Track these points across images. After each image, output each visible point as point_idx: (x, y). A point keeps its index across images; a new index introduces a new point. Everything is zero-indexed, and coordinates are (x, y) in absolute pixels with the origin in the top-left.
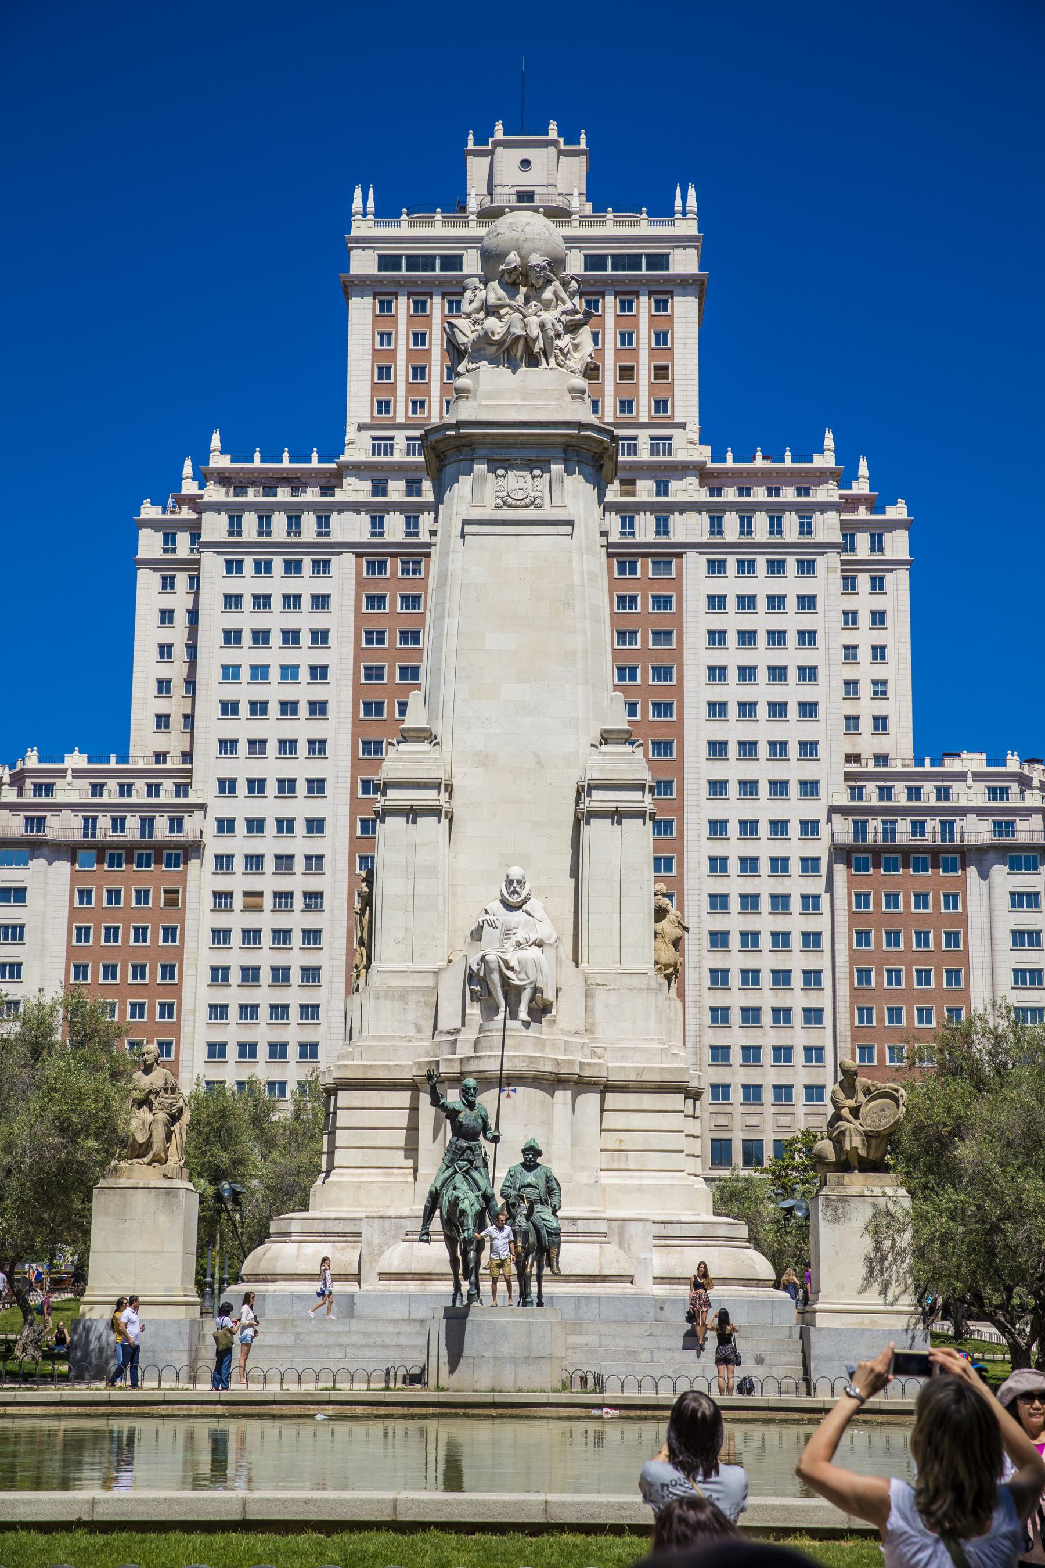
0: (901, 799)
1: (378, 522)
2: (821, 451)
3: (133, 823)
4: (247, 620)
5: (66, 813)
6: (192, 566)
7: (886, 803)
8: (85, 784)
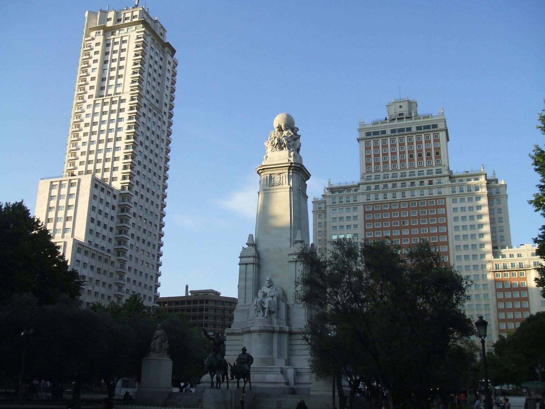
4: (338, 224)
6: (325, 212)
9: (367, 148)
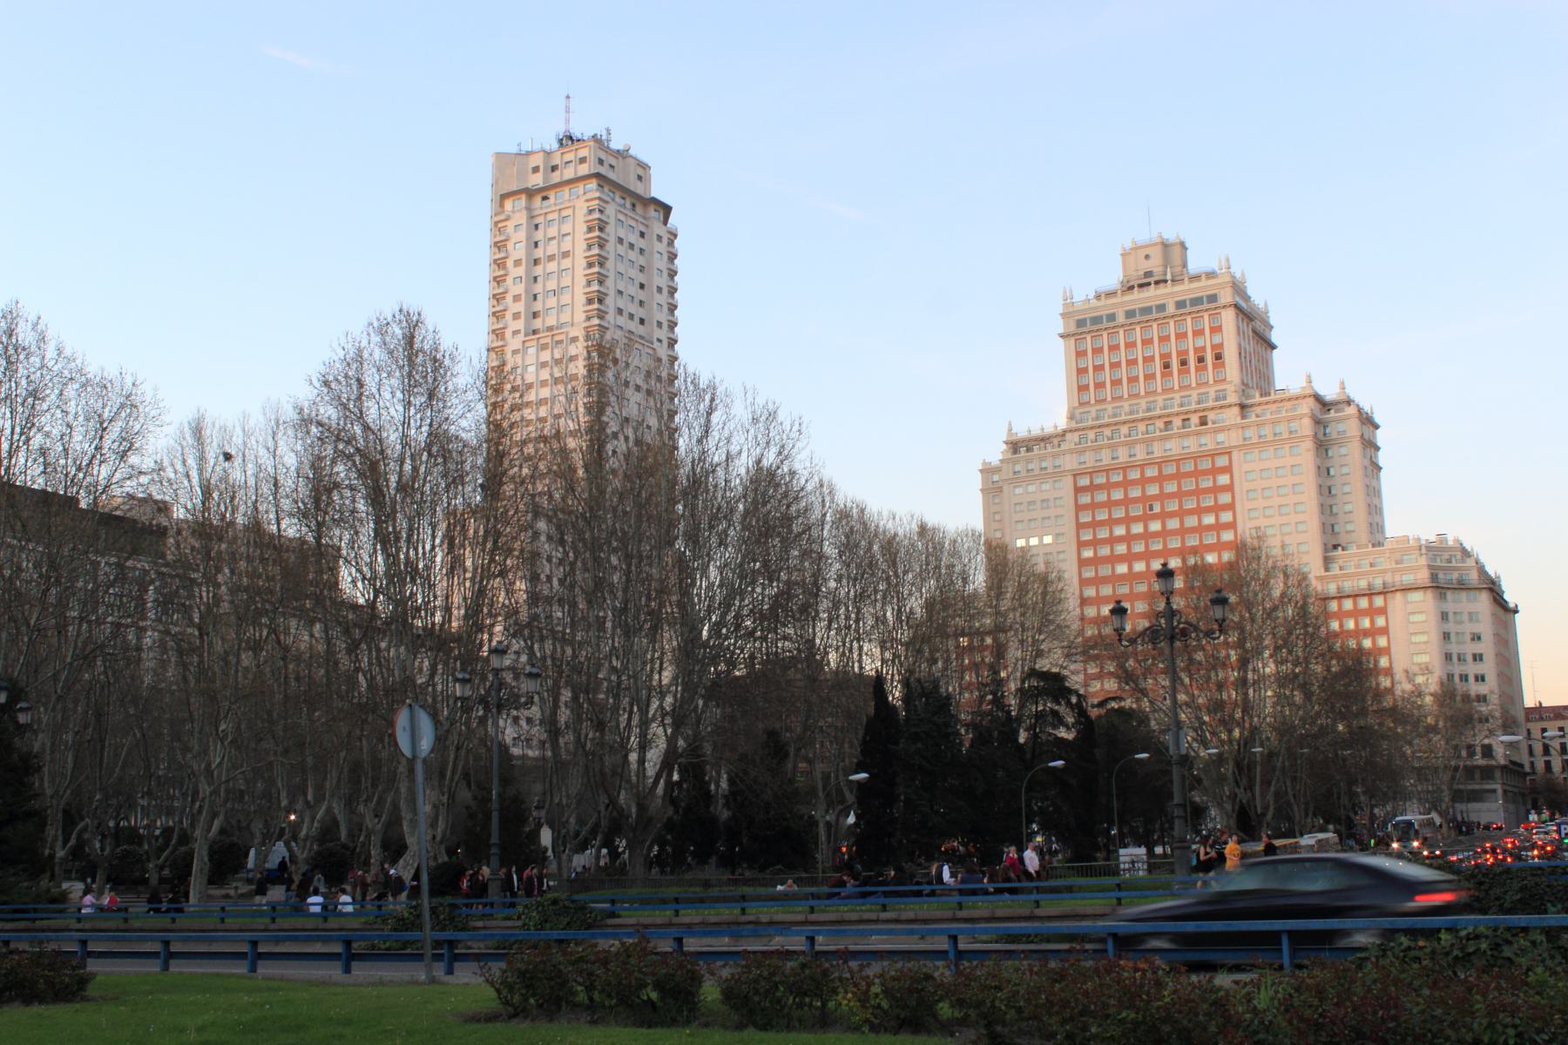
9: (1080, 354)
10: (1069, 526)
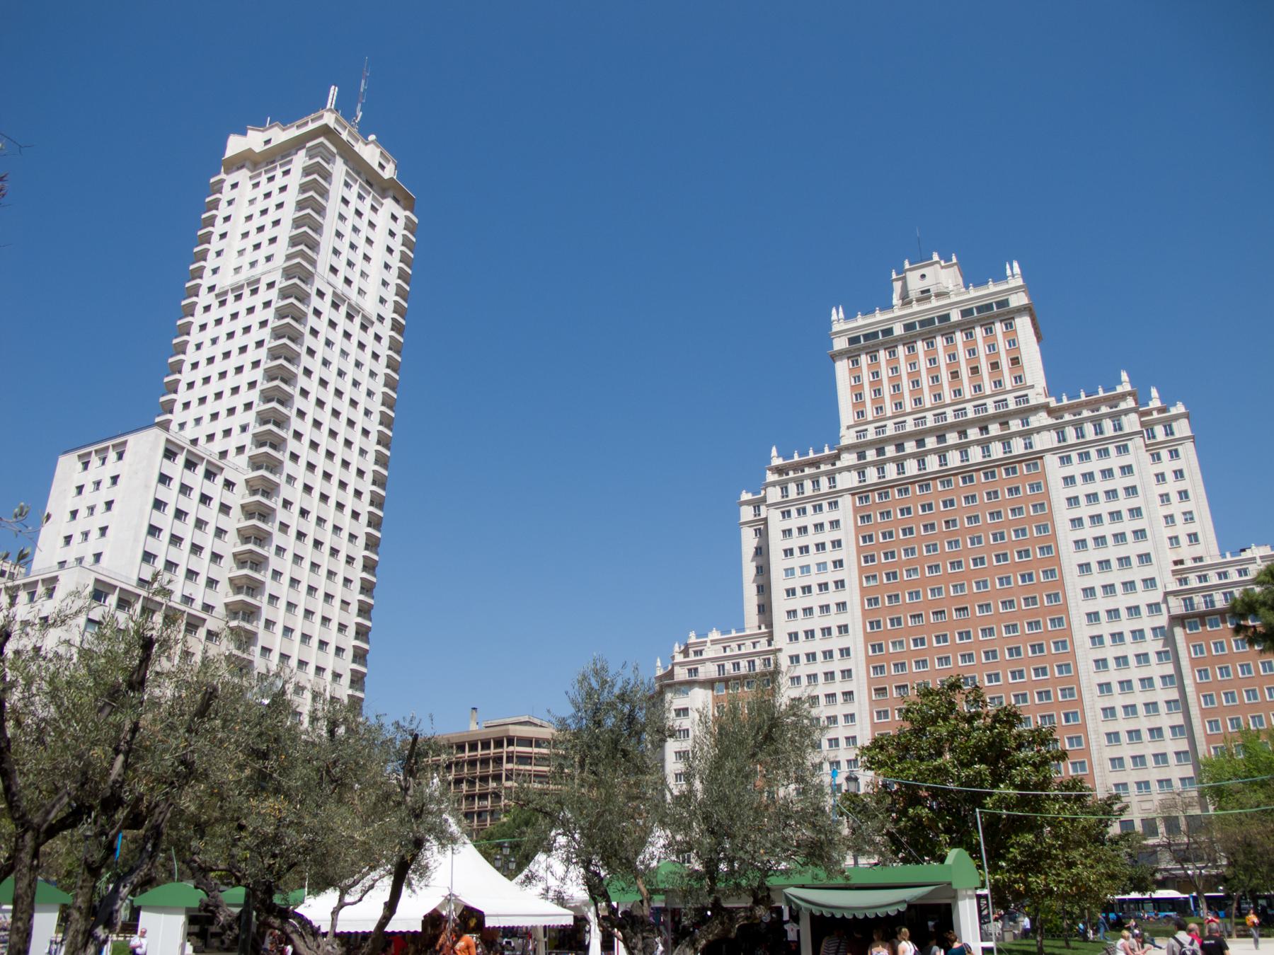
0: (1214, 579)
1: (862, 474)
2: (1120, 383)
3: (744, 663)
5: (709, 664)
7: (1204, 584)
8: (719, 647)
10: (849, 554)
